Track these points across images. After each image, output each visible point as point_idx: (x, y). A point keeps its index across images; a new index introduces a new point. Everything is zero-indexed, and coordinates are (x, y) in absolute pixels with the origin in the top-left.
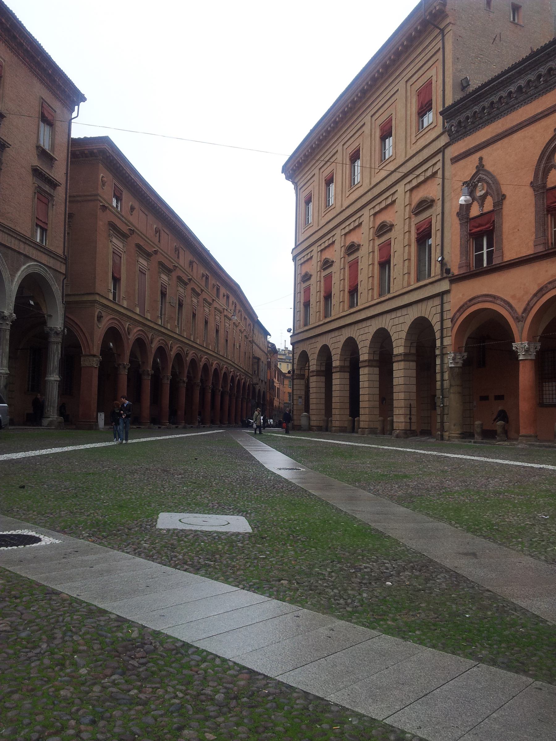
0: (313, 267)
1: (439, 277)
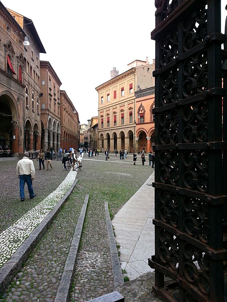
0: (104, 114)
1: (134, 123)
